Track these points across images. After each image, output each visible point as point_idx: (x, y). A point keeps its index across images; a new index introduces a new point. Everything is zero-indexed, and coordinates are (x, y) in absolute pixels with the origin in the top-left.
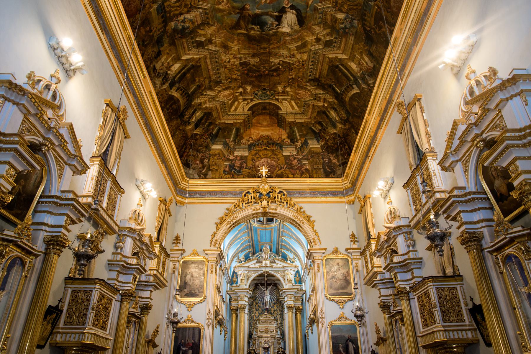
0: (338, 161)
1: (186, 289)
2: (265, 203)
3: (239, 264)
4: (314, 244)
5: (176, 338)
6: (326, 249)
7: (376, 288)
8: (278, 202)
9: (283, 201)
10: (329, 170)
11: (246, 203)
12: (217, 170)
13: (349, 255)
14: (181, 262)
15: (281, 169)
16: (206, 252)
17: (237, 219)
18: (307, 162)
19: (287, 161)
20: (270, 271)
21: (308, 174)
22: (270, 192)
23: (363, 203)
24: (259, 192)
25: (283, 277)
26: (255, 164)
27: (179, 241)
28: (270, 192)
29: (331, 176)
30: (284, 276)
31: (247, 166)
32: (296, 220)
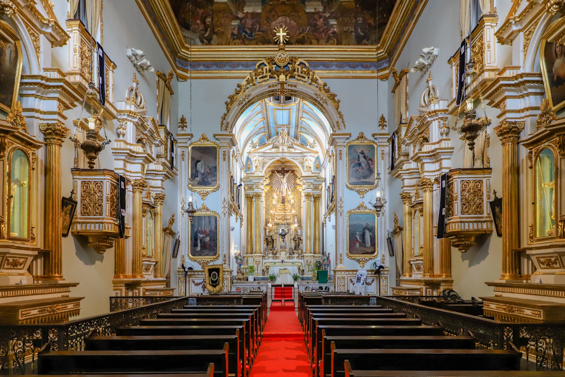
0: (375, 21)
1: (198, 177)
2: (282, 77)
3: (253, 149)
4: (338, 128)
5: (192, 226)
6: (350, 135)
7: (400, 178)
8: (299, 76)
9: (303, 75)
10: (362, 34)
11: (260, 78)
12: (223, 33)
13: (376, 141)
14: (190, 148)
15: (303, 32)
16: (216, 137)
17: (250, 98)
18: (336, 23)
19: (311, 21)
20: (287, 158)
21: (335, 40)
22: (289, 63)
23: (398, 80)
24: (275, 64)
25: (302, 163)
26: (270, 26)
27: (185, 124)
28: (289, 63)
29: (363, 41)
30: (303, 163)
31: (260, 28)
32: (319, 99)
